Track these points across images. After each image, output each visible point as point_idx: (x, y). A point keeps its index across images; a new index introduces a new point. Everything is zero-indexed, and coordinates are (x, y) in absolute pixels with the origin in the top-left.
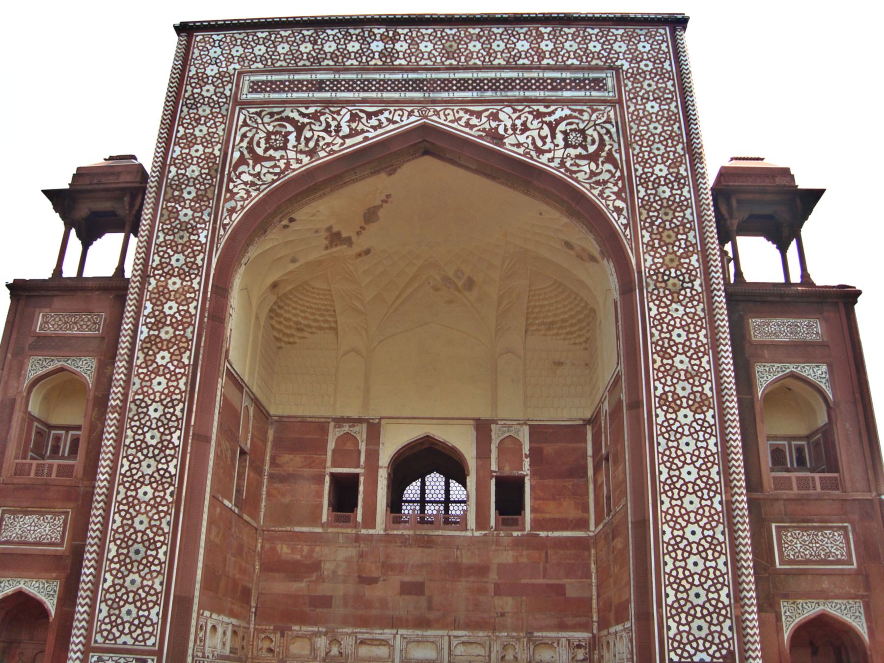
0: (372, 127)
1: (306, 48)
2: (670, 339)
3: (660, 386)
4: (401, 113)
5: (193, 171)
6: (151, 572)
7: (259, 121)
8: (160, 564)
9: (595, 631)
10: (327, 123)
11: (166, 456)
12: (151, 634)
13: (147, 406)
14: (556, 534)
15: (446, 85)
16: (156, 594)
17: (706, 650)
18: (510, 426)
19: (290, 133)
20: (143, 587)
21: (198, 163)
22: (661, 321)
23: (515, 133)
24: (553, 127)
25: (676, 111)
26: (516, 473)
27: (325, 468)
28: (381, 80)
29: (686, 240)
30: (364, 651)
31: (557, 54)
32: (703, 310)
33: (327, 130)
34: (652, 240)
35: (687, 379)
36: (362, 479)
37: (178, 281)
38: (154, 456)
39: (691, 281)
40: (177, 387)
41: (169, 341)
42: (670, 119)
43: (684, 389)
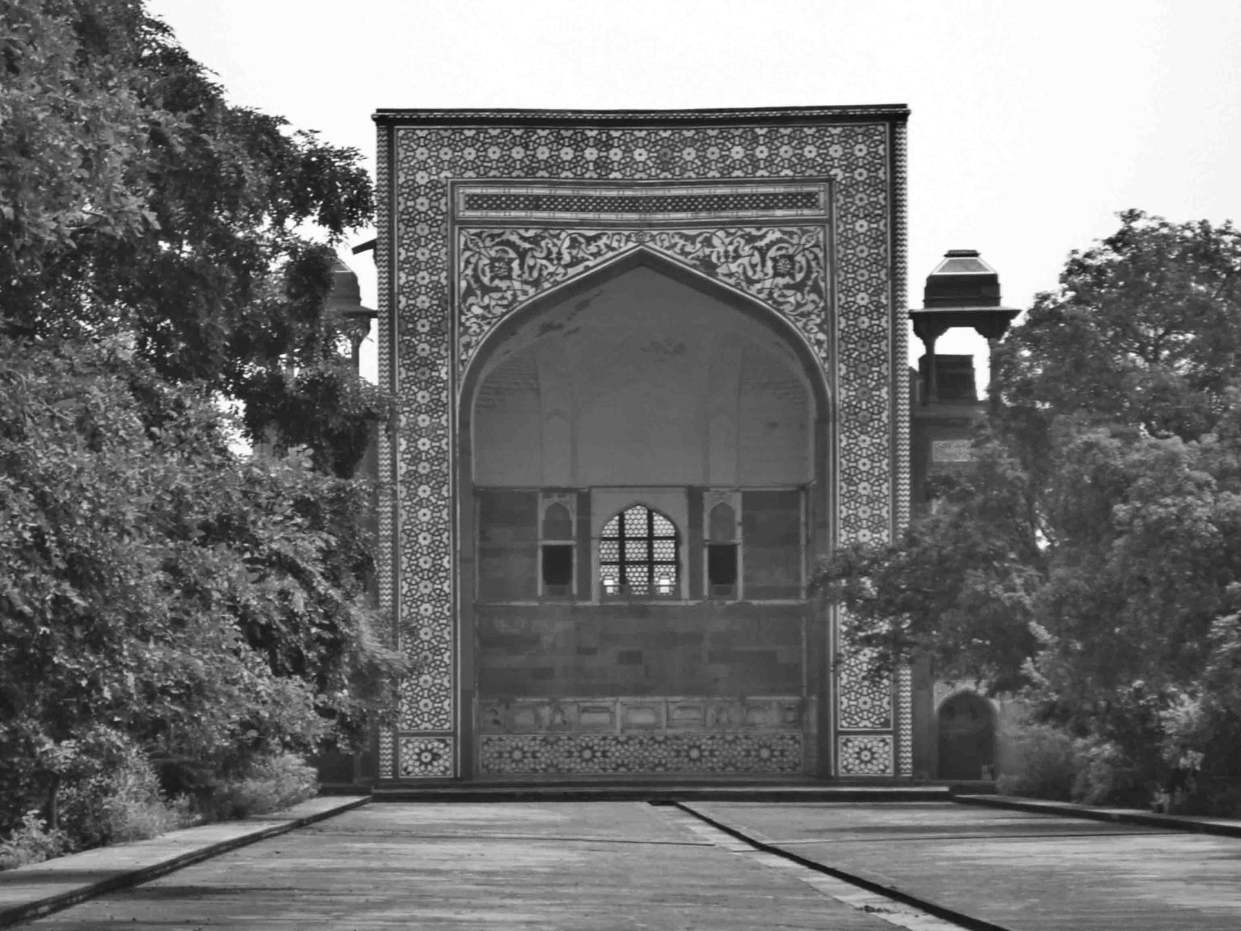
0: (592, 254)
1: (518, 153)
2: (856, 468)
4: (617, 237)
5: (423, 302)
6: (439, 673)
7: (481, 245)
8: (446, 666)
9: (805, 694)
10: (549, 249)
11: (439, 578)
12: (446, 720)
13: (417, 535)
15: (661, 204)
18: (723, 493)
19: (512, 260)
20: (434, 685)
24: (763, 252)
27: (537, 540)
28: (598, 198)
29: (879, 372)
30: (587, 718)
32: (888, 441)
33: (547, 258)
34: (848, 373)
35: (867, 504)
36: (575, 552)
37: (428, 419)
38: (429, 579)
39: (880, 413)
40: (440, 518)
41: (427, 476)
42: (877, 240)
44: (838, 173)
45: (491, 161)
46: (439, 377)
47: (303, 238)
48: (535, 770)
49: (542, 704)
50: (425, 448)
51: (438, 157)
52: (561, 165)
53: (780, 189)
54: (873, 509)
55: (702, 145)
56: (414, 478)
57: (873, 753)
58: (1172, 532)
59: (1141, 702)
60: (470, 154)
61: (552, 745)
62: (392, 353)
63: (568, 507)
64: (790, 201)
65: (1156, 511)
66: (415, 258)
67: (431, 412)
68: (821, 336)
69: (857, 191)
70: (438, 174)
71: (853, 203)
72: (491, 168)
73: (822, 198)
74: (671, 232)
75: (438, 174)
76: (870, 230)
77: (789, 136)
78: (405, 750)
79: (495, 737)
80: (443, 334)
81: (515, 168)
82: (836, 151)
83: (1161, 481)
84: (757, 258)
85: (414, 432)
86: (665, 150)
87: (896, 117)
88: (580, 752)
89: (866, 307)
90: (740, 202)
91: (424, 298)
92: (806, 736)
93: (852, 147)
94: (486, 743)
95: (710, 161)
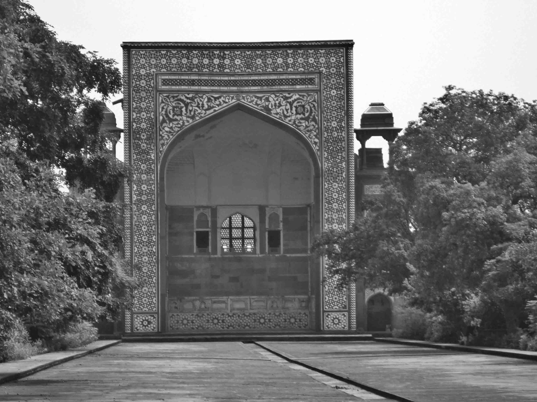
1: (184, 61)
3: (326, 215)
5: (144, 125)
6: (151, 286)
7: (168, 100)
10: (198, 102)
11: (151, 245)
12: (154, 307)
13: (141, 227)
14: (294, 255)
15: (247, 83)
16: (154, 293)
17: (337, 305)
18: (274, 208)
19: (183, 107)
21: (145, 122)
22: (329, 190)
23: (276, 108)
24: (291, 104)
25: (343, 94)
26: (277, 229)
27: (193, 229)
29: (341, 156)
30: (215, 306)
31: (295, 65)
33: (198, 106)
34: (328, 156)
35: (337, 212)
36: (210, 233)
37: (146, 176)
38: (147, 245)
39: (342, 173)
40: (151, 219)
41: (146, 201)
43: (335, 216)
44: (324, 70)
45: (173, 64)
46: (150, 158)
47: (92, 98)
48: (193, 328)
49: (196, 300)
50: (145, 189)
51: (149, 63)
52: (203, 66)
53: (298, 77)
54: (339, 214)
55: (264, 58)
56: (140, 202)
57: (339, 320)
58: (467, 224)
59: (455, 297)
60: (164, 61)
61: (200, 317)
62: (130, 148)
63: (207, 214)
64: (303, 82)
65: (461, 215)
66: (140, 106)
67: (147, 173)
68: (317, 140)
69: (332, 77)
70: (150, 70)
71: (330, 83)
72: (173, 67)
73: (317, 80)
74: (251, 95)
75: (150, 70)
76: (337, 94)
77: (302, 54)
78: (136, 320)
79: (175, 314)
80: (152, 139)
81: (183, 68)
82: (322, 60)
83: (462, 202)
84: (288, 107)
85: (140, 182)
86: (248, 60)
87: (348, 45)
88: (212, 320)
89: (336, 128)
90: (281, 82)
91: (144, 124)
92: (310, 313)
93: (329, 58)
94: (172, 317)
95: (268, 64)
